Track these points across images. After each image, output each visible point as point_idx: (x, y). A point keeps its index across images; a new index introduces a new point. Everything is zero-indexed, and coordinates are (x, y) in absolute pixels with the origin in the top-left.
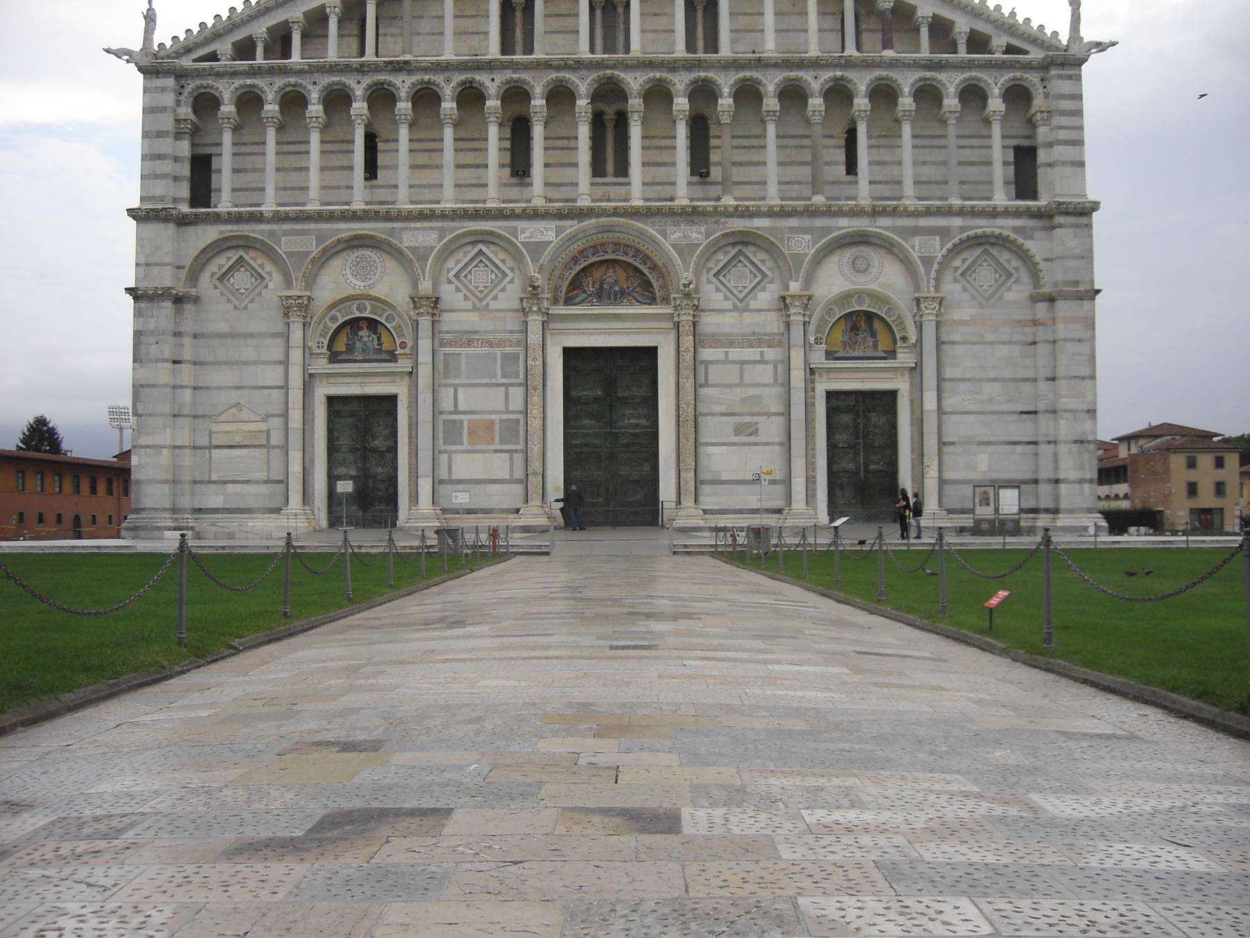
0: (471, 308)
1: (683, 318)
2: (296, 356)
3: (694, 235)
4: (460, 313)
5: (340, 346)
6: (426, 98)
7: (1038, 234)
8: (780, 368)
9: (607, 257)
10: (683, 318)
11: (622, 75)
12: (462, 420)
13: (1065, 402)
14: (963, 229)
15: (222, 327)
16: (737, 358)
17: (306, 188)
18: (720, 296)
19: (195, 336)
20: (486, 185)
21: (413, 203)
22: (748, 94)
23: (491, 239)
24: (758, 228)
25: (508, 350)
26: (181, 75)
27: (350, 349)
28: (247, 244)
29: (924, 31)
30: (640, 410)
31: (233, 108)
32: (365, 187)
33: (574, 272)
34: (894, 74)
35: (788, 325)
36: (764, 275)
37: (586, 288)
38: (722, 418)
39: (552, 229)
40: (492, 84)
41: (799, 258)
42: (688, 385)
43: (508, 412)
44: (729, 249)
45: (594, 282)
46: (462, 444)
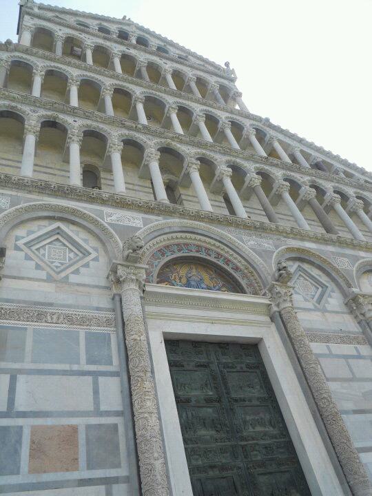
0: (45, 278)
1: (282, 306)
3: (266, 245)
4: (31, 282)
10: (282, 306)
12: (21, 427)
23: (73, 218)
24: (310, 248)
25: (95, 329)
30: (262, 415)
36: (324, 287)
37: (173, 282)
38: (357, 416)
43: (98, 413)
45: (180, 278)
46: (18, 473)
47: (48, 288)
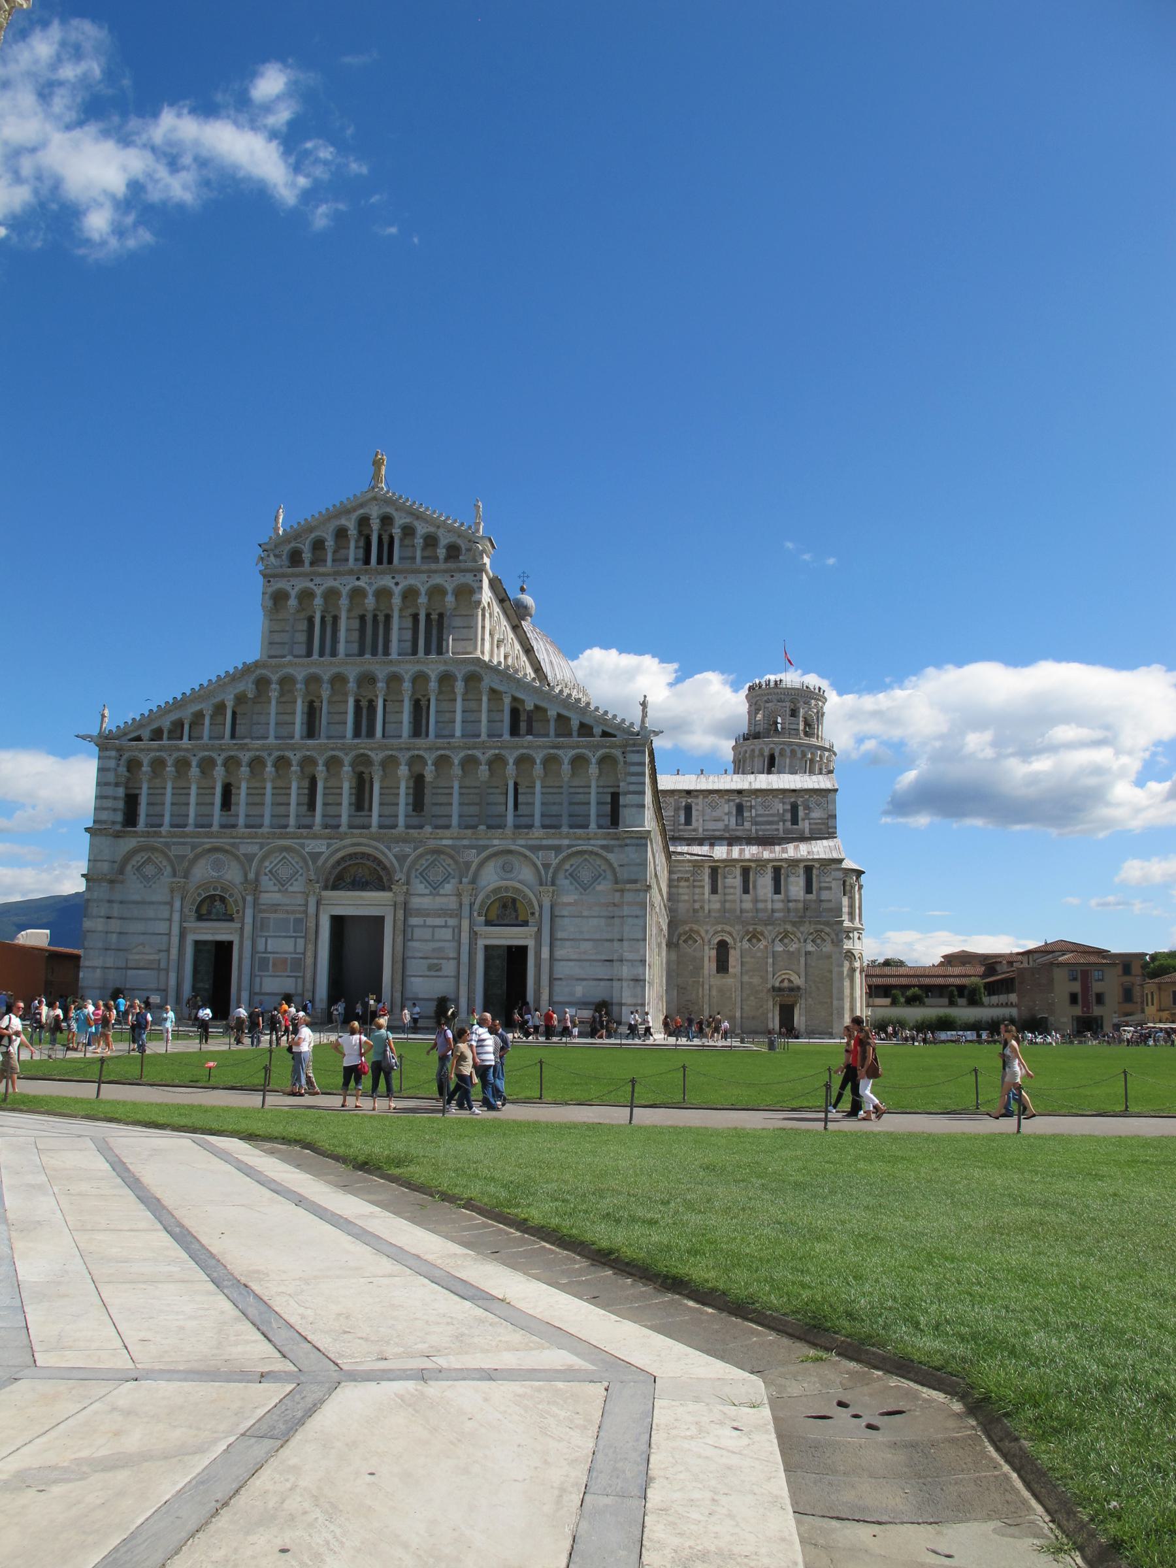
2: (176, 917)
5: (204, 911)
6: (256, 764)
7: (616, 850)
8: (456, 930)
9: (357, 861)
11: (370, 753)
13: (628, 955)
14: (569, 846)
15: (136, 897)
16: (431, 924)
17: (188, 816)
18: (422, 886)
19: (121, 902)
20: (289, 816)
21: (247, 826)
22: (442, 762)
25: (298, 916)
26: (120, 751)
27: (209, 913)
28: (154, 849)
29: (552, 724)
31: (149, 769)
32: (221, 816)
33: (337, 871)
34: (531, 752)
35: (461, 905)
36: (450, 874)
39: (322, 845)
40: (296, 759)
41: (468, 865)
42: (400, 939)
44: (428, 857)
47: (278, 896)
